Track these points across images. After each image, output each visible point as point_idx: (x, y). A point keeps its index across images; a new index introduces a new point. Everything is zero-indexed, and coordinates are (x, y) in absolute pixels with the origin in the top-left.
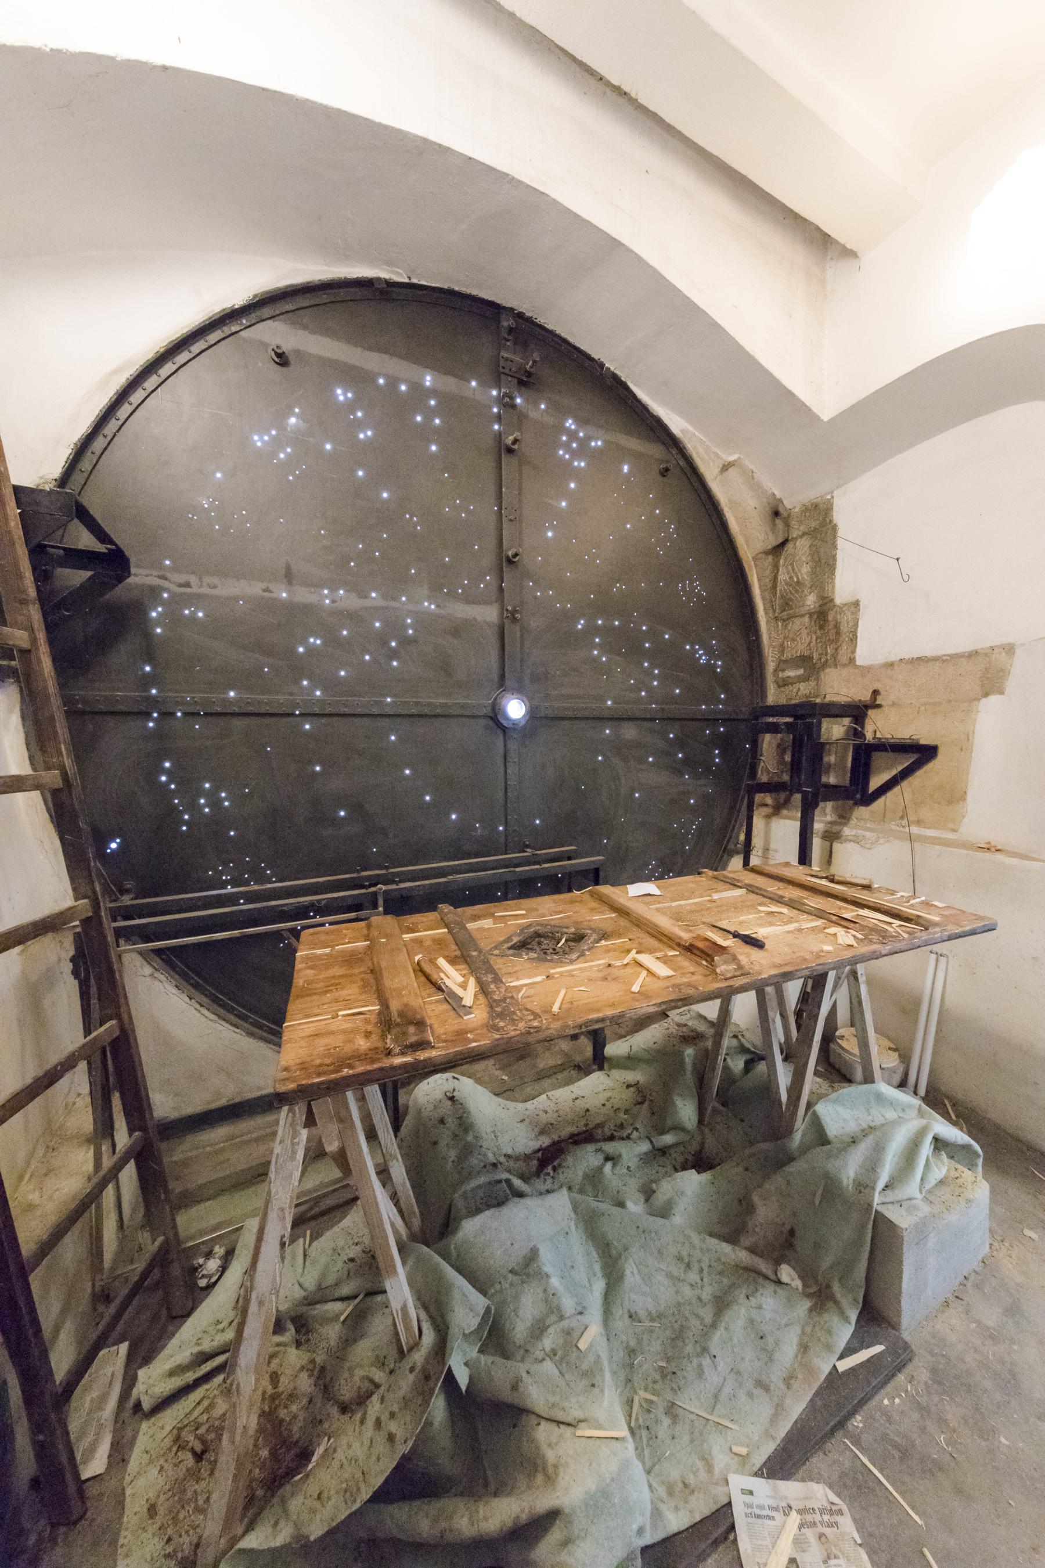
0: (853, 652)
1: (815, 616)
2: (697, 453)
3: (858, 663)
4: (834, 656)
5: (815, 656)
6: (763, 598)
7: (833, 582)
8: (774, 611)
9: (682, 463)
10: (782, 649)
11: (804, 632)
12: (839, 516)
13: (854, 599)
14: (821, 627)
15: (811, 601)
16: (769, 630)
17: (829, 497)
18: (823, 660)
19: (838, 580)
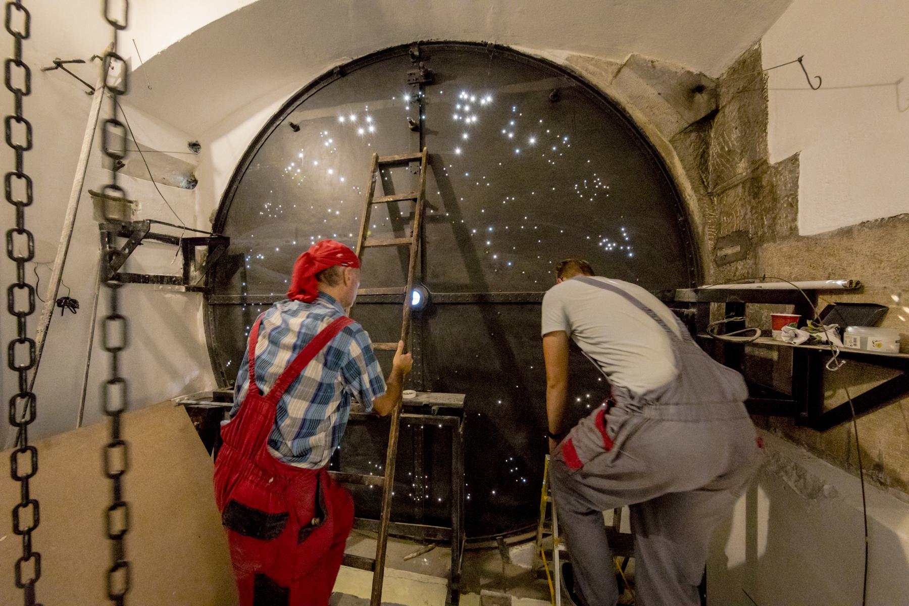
1: (748, 185)
3: (802, 233)
4: (772, 227)
6: (690, 177)
8: (706, 188)
11: (739, 203)
14: (756, 195)
15: (742, 168)
18: (759, 233)
19: (770, 139)
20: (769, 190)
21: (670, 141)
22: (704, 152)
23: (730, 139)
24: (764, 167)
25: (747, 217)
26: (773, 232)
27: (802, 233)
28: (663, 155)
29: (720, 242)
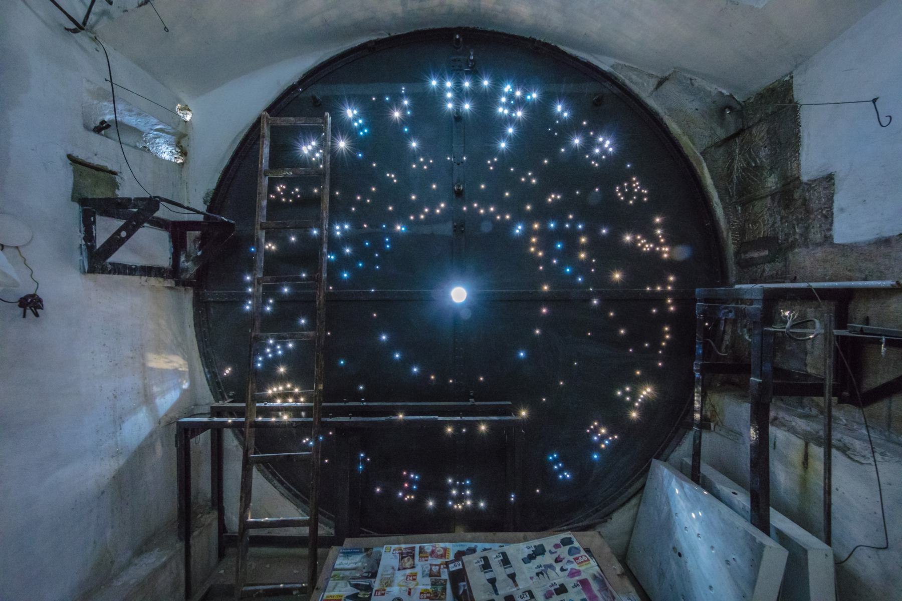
0: (830, 230)
1: (777, 197)
2: (630, 79)
3: (837, 240)
4: (805, 235)
5: (781, 237)
6: (716, 186)
7: (798, 159)
9: (616, 90)
10: (742, 232)
12: (800, 94)
13: (825, 174)
15: (772, 182)
16: (726, 214)
17: (787, 78)
18: (790, 240)
19: (803, 158)
20: (803, 203)
21: (701, 153)
22: (730, 165)
23: (758, 156)
24: (797, 182)
25: (776, 225)
26: (806, 239)
27: (837, 240)
28: (695, 165)
29: (744, 246)
